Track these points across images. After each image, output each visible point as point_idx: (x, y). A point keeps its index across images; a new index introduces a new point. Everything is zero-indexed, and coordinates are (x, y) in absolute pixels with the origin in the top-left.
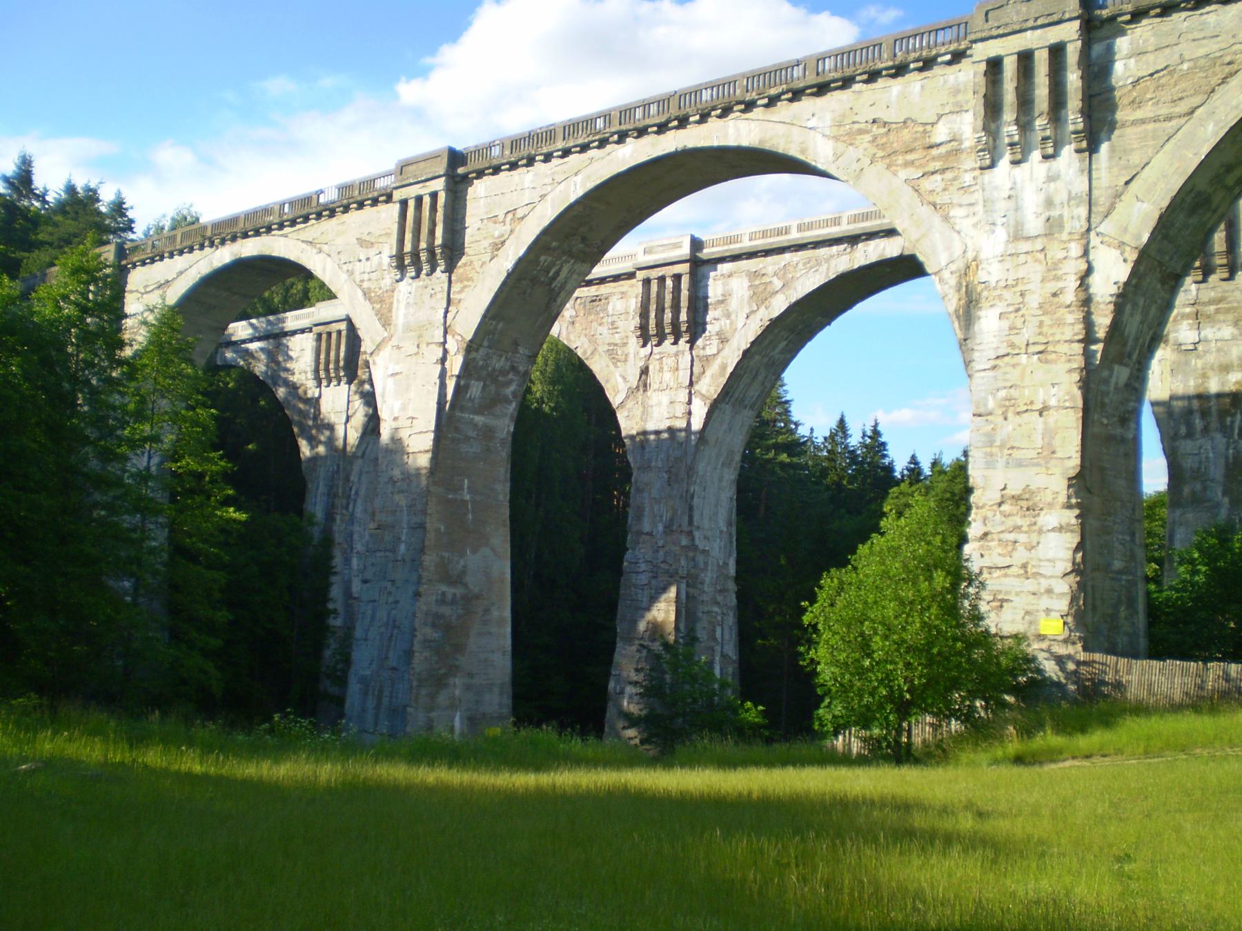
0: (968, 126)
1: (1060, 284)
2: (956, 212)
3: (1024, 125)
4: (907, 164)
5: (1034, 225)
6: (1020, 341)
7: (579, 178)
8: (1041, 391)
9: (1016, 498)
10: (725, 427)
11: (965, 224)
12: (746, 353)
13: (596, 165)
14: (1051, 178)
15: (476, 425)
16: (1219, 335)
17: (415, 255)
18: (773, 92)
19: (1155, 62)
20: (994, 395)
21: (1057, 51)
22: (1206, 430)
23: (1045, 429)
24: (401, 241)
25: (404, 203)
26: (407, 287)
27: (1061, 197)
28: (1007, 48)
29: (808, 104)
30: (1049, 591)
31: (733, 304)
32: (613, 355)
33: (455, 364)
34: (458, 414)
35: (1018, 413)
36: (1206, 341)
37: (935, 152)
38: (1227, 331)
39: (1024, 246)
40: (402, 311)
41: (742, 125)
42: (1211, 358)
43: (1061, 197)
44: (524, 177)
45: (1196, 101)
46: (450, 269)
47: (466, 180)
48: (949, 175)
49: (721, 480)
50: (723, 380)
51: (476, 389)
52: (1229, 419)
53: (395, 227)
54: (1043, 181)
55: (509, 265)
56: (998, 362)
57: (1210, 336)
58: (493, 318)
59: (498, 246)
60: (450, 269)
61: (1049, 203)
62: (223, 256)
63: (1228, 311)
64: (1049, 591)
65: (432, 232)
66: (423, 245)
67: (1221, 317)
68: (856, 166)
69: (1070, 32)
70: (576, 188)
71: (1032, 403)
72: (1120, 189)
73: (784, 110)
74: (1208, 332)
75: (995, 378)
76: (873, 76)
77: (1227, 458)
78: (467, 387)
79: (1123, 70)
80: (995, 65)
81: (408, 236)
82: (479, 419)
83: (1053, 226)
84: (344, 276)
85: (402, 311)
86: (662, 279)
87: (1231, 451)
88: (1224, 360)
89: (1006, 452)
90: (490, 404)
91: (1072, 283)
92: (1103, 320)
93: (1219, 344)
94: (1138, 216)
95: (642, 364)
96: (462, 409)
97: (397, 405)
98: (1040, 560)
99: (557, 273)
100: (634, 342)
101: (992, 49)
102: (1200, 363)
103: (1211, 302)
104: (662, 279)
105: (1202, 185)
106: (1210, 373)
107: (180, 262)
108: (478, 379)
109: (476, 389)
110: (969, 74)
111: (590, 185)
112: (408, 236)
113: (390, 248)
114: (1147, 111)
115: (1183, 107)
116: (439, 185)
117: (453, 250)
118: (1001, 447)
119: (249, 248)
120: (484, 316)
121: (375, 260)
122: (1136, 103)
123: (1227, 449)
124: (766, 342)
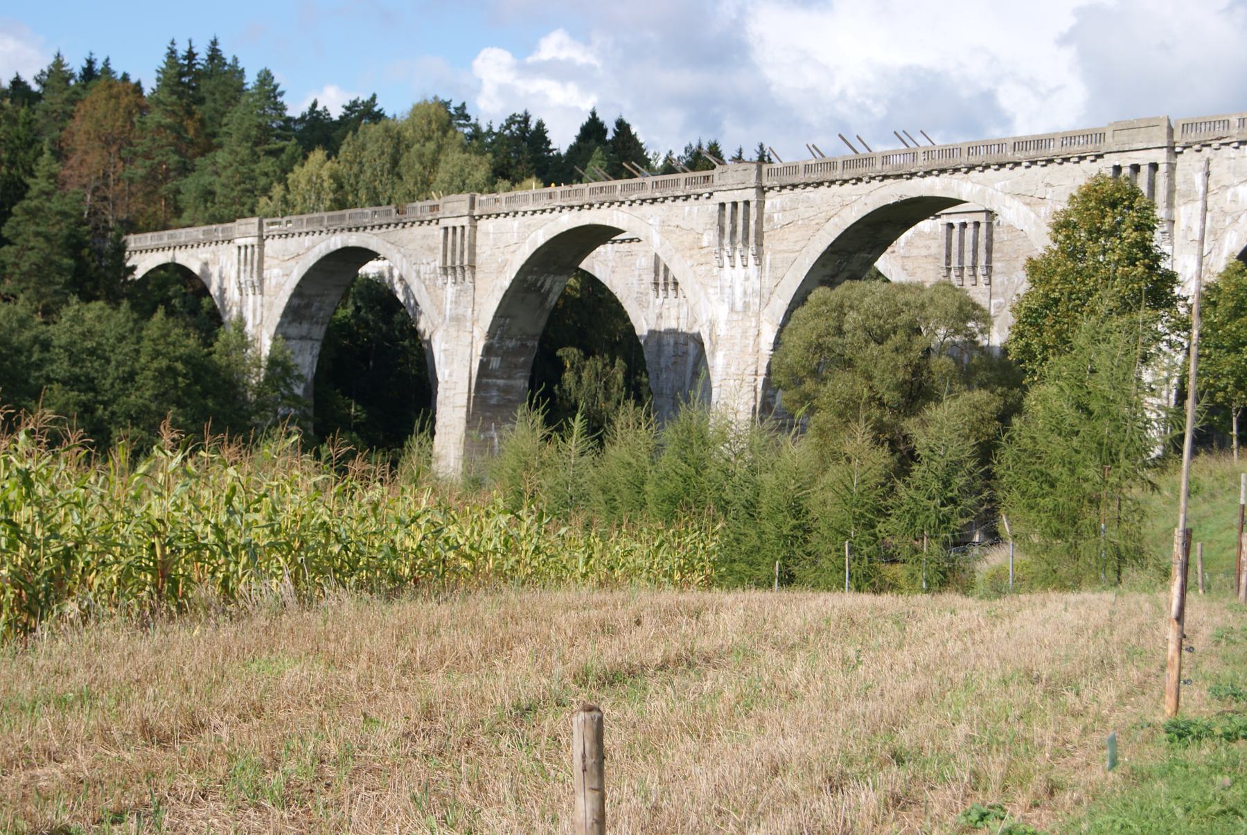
2: (711, 291)
3: (732, 242)
4: (691, 257)
5: (739, 305)
7: (541, 232)
11: (714, 298)
13: (550, 225)
14: (747, 279)
15: (498, 386)
17: (454, 268)
18: (633, 198)
21: (747, 203)
24: (445, 256)
25: (446, 229)
26: (450, 290)
27: (749, 291)
28: (728, 197)
34: (485, 380)
37: (704, 251)
39: (735, 317)
40: (448, 307)
41: (620, 214)
43: (749, 291)
44: (513, 224)
45: (803, 243)
48: (708, 267)
51: (495, 363)
53: (441, 246)
55: (507, 284)
58: (501, 317)
59: (501, 269)
61: (745, 293)
65: (462, 253)
66: (458, 263)
78: (488, 362)
80: (723, 205)
81: (449, 254)
82: (501, 382)
83: (746, 306)
84: (414, 274)
85: (448, 307)
95: (657, 311)
96: (488, 376)
97: (447, 372)
100: (652, 294)
101: (719, 197)
107: (307, 240)
108: (497, 356)
111: (549, 237)
112: (449, 254)
113: (439, 263)
115: (798, 248)
116: (465, 221)
120: (495, 317)
121: (432, 264)
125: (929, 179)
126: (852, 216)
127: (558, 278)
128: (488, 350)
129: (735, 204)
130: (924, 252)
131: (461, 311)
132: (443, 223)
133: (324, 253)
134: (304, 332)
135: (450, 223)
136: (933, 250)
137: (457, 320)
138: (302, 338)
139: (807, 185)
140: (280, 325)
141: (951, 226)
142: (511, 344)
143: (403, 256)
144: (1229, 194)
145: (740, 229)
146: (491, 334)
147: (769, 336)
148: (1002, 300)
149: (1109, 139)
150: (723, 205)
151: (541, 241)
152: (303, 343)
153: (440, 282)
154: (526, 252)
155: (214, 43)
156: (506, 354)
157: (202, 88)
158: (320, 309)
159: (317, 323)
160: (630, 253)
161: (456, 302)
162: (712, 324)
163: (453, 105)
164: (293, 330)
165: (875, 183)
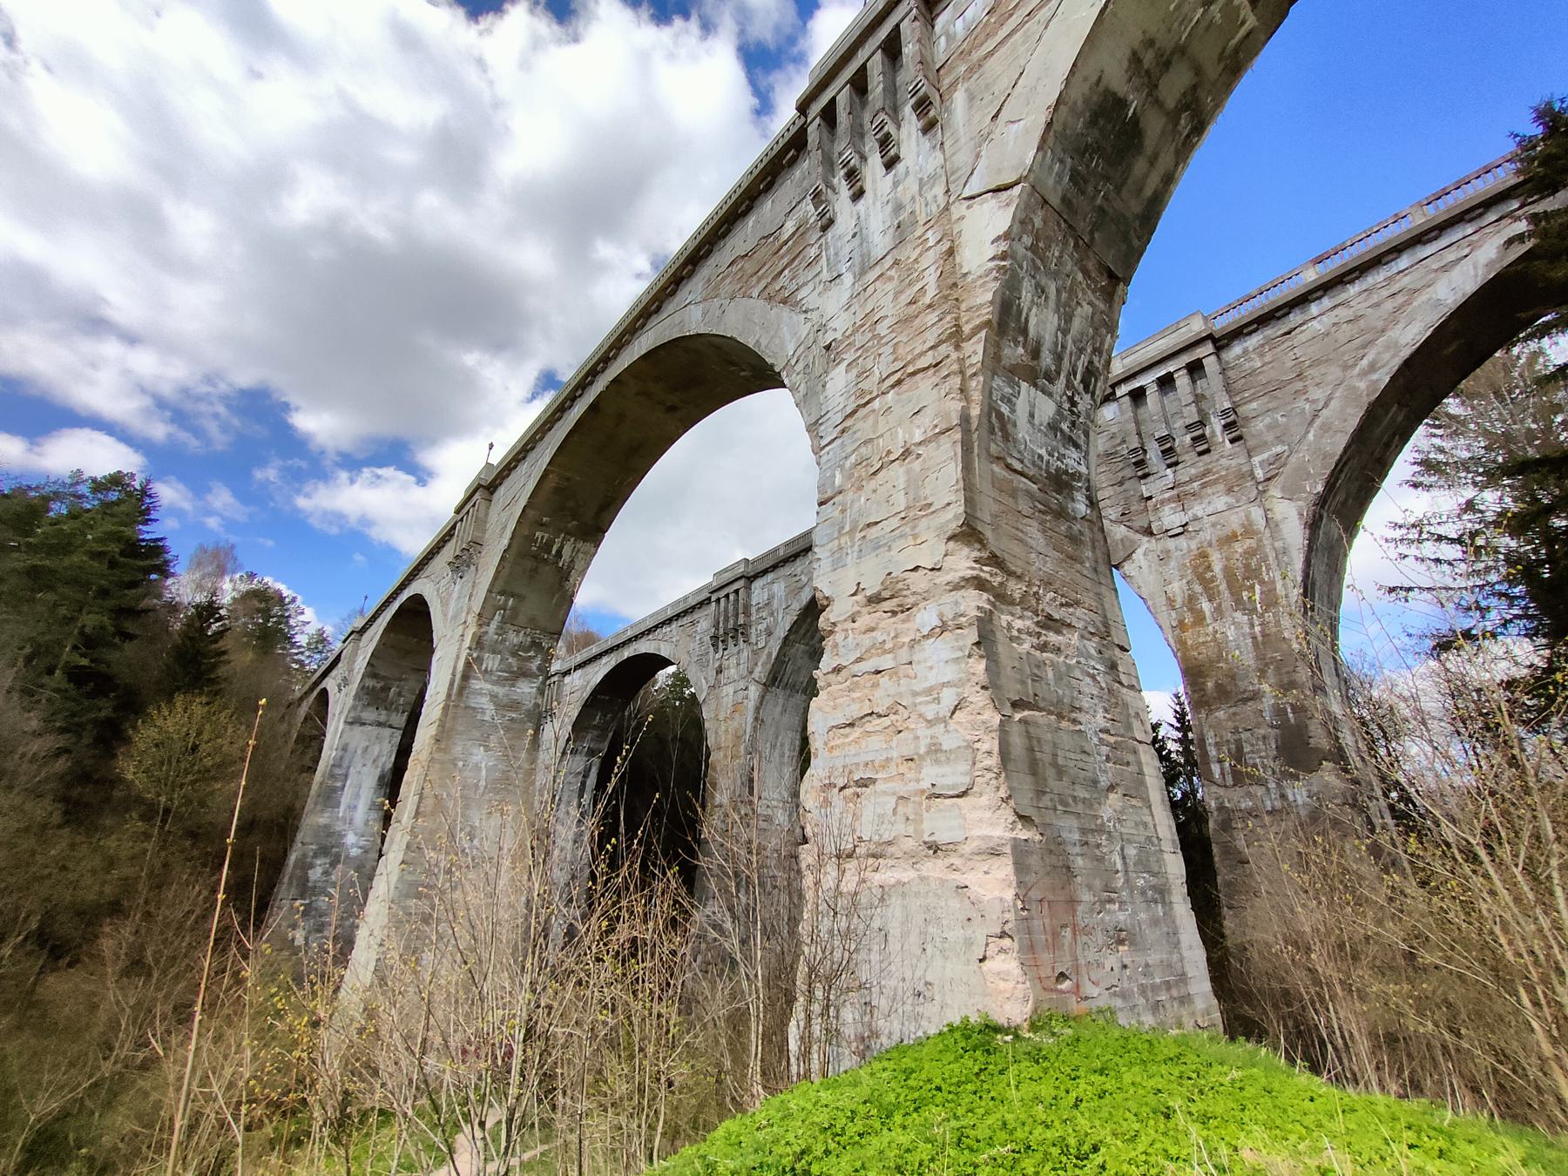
1: (919, 286)
5: (880, 242)
6: (870, 384)
8: (900, 431)
9: (875, 600)
10: (779, 709)
12: (786, 638)
14: (896, 184)
16: (1210, 510)
20: (842, 467)
22: (1218, 611)
23: (908, 481)
30: (935, 750)
31: (775, 603)
35: (874, 474)
36: (1196, 519)
38: (1221, 502)
42: (1207, 535)
49: (782, 755)
50: (769, 666)
52: (1245, 594)
55: (506, 541)
56: (848, 423)
57: (1200, 514)
58: (502, 593)
61: (898, 208)
62: (396, 606)
63: (1215, 482)
64: (935, 750)
67: (1209, 491)
68: (718, 313)
71: (889, 452)
72: (985, 132)
74: (1198, 509)
75: (843, 445)
77: (1254, 638)
78: (479, 660)
86: (727, 596)
87: (1257, 629)
88: (1227, 531)
89: (859, 535)
91: (931, 278)
93: (1212, 518)
98: (915, 694)
99: (559, 554)
102: (1194, 545)
103: (1191, 481)
104: (727, 596)
105: (1118, 82)
106: (1209, 550)
108: (494, 652)
118: (852, 531)
120: (490, 591)
123: (1252, 626)
124: (802, 631)
127: (580, 545)
128: (479, 643)
134: (383, 718)
137: (455, 617)
138: (380, 724)
140: (354, 708)
146: (483, 618)
148: (1279, 449)
152: (380, 730)
158: (399, 694)
159: (397, 710)
164: (370, 715)
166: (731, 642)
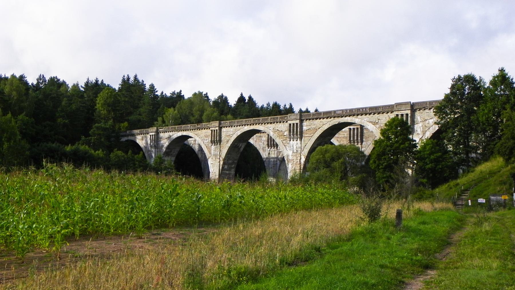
0: (287, 133)
3: (293, 135)
5: (295, 151)
11: (288, 149)
14: (297, 144)
17: (214, 141)
19: (309, 127)
21: (297, 124)
26: (213, 147)
29: (269, 125)
32: (264, 150)
33: (222, 163)
44: (231, 129)
46: (220, 145)
47: (222, 127)
51: (226, 167)
54: (295, 144)
59: (228, 141)
60: (220, 145)
69: (298, 121)
70: (239, 133)
73: (267, 126)
76: (277, 123)
79: (305, 128)
80: (290, 124)
82: (227, 172)
90: (229, 169)
92: (302, 167)
94: (306, 151)
100: (267, 147)
107: (171, 134)
109: (226, 167)
110: (287, 125)
113: (210, 140)
114: (307, 135)
116: (217, 128)
117: (220, 141)
119: (185, 133)
122: (307, 134)
125: (347, 118)
126: (326, 127)
129: (294, 124)
130: (343, 136)
131: (216, 153)
132: (211, 129)
133: (176, 137)
135: (213, 129)
136: (346, 135)
137: (215, 155)
139: (313, 119)
141: (350, 129)
142: (230, 162)
143: (199, 138)
144: (427, 122)
145: (295, 131)
147: (303, 159)
149: (395, 108)
150: (290, 124)
151: (239, 134)
153: (210, 145)
154: (235, 137)
155: (136, 76)
156: (229, 164)
157: (133, 88)
160: (260, 137)
161: (215, 150)
162: (288, 156)
163: (203, 94)
165: (332, 119)
166: (273, 148)
